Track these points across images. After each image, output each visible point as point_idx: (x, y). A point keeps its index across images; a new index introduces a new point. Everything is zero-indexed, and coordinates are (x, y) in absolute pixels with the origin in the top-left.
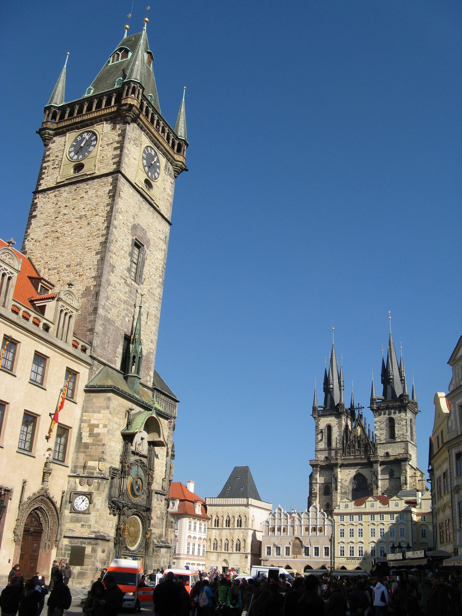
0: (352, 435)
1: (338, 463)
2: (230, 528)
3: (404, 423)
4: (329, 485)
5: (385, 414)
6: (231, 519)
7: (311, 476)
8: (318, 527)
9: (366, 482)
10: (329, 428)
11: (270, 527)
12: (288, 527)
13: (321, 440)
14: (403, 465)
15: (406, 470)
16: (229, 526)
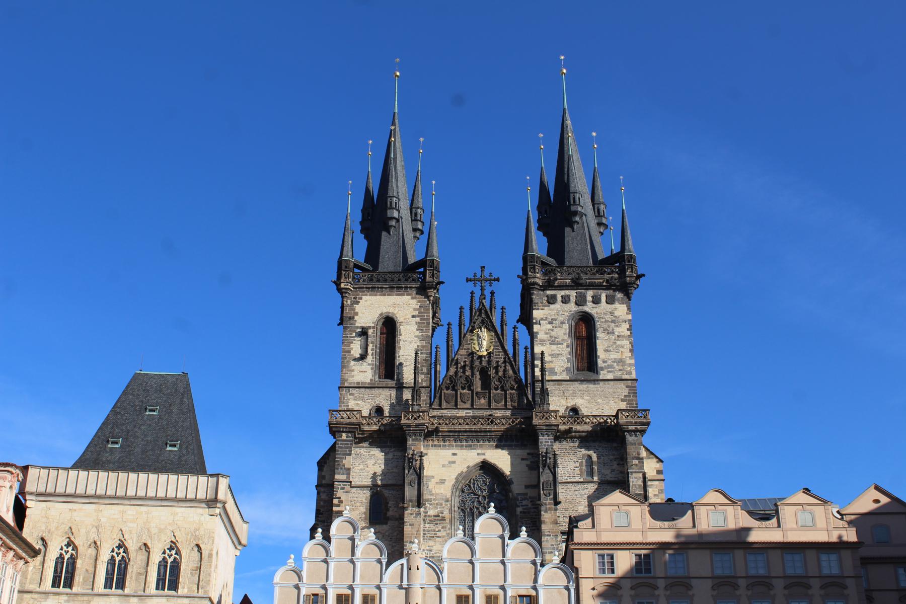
0: (463, 352)
1: (423, 425)
2: (127, 591)
3: (623, 329)
4: (387, 493)
5: (566, 300)
6: (132, 555)
7: (328, 464)
8: (510, 593)
9: (510, 491)
10: (389, 325)
11: (304, 591)
12: (385, 591)
13: (363, 357)
14: (632, 444)
15: (641, 460)
16: (121, 585)
